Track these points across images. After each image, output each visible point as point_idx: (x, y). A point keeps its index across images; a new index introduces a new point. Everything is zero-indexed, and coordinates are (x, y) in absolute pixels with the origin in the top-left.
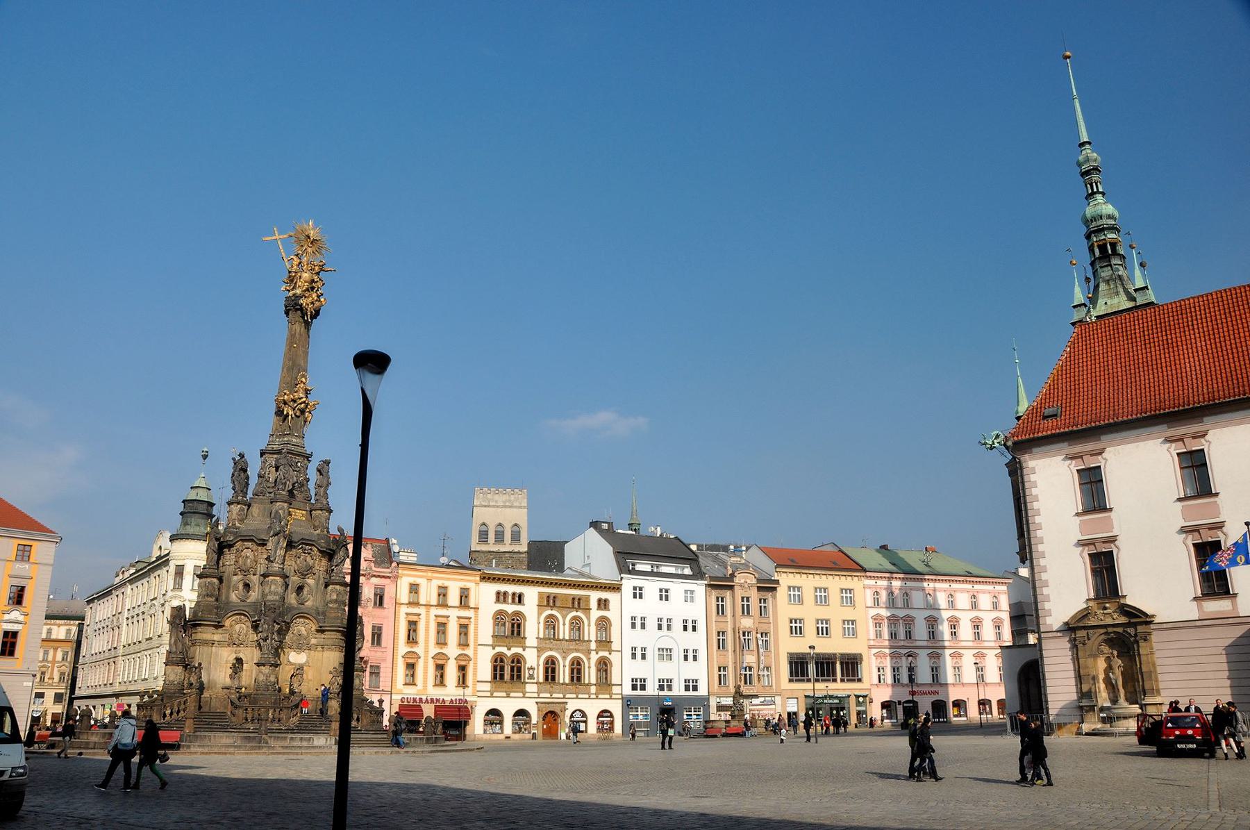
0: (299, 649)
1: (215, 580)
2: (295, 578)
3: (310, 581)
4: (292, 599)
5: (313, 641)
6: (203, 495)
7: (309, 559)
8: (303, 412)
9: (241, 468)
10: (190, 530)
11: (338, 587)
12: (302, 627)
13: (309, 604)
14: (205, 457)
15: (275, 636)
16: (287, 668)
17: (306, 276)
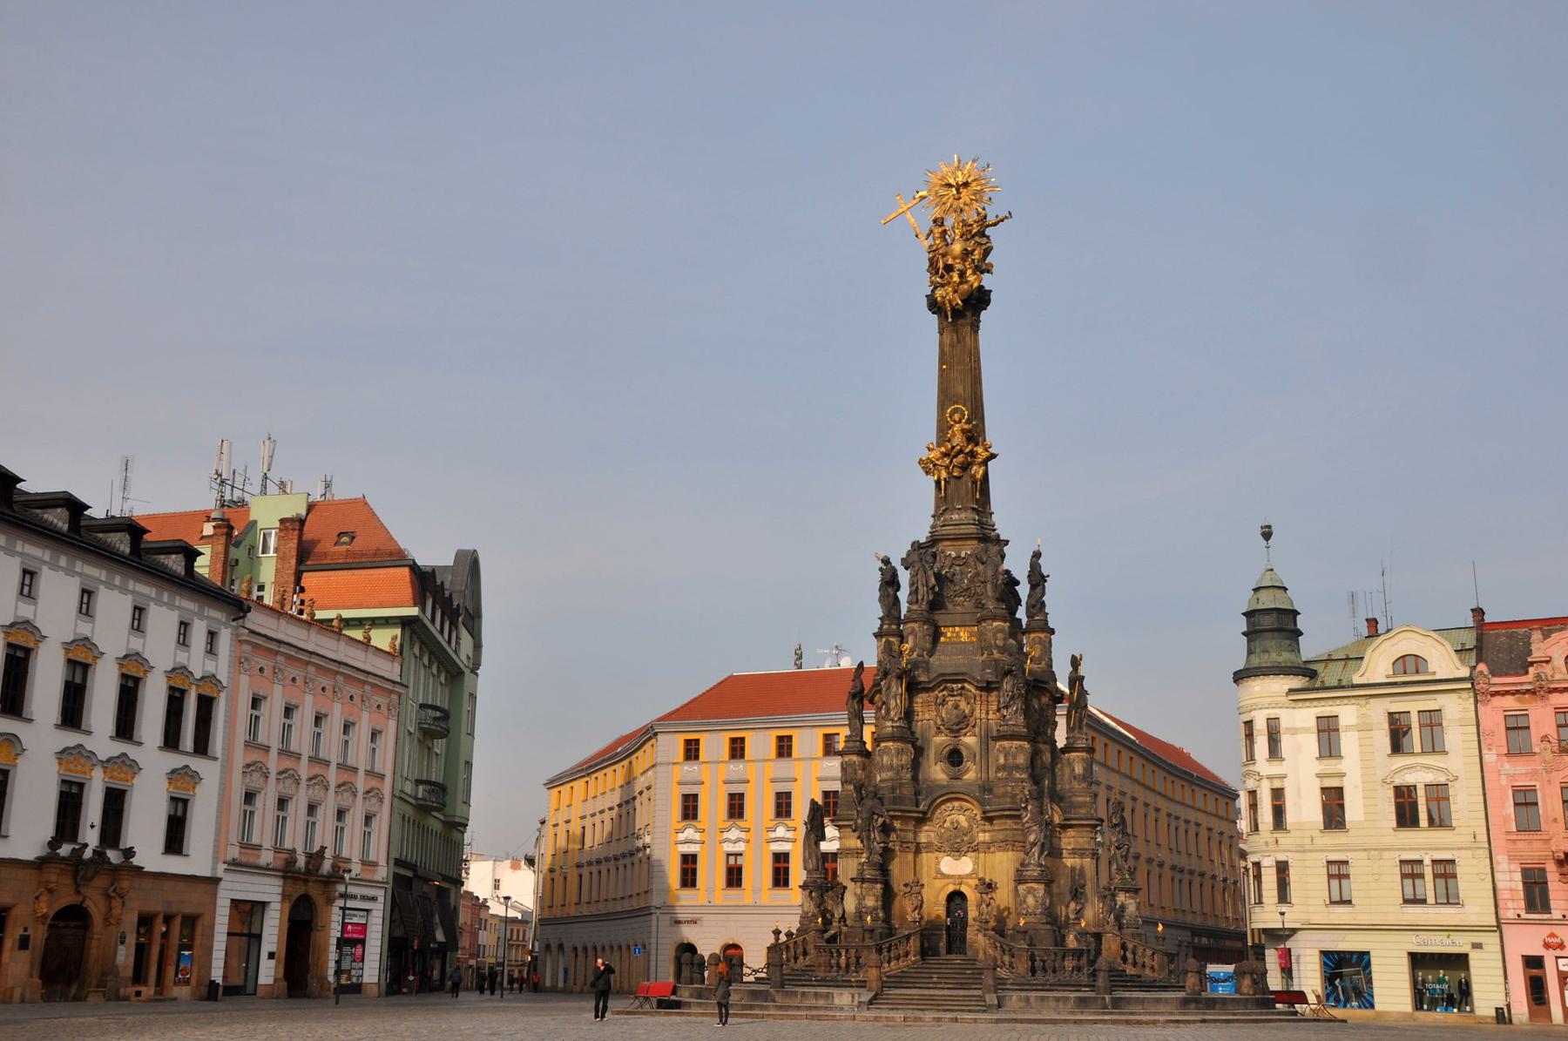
0: (957, 851)
1: (855, 758)
2: (941, 739)
3: (970, 740)
4: (937, 772)
5: (983, 837)
6: (1268, 601)
7: (963, 705)
8: (965, 467)
9: (890, 582)
10: (1256, 661)
11: (1006, 744)
12: (958, 815)
13: (970, 776)
14: (1267, 535)
15: (876, 835)
16: (938, 883)
17: (957, 248)
